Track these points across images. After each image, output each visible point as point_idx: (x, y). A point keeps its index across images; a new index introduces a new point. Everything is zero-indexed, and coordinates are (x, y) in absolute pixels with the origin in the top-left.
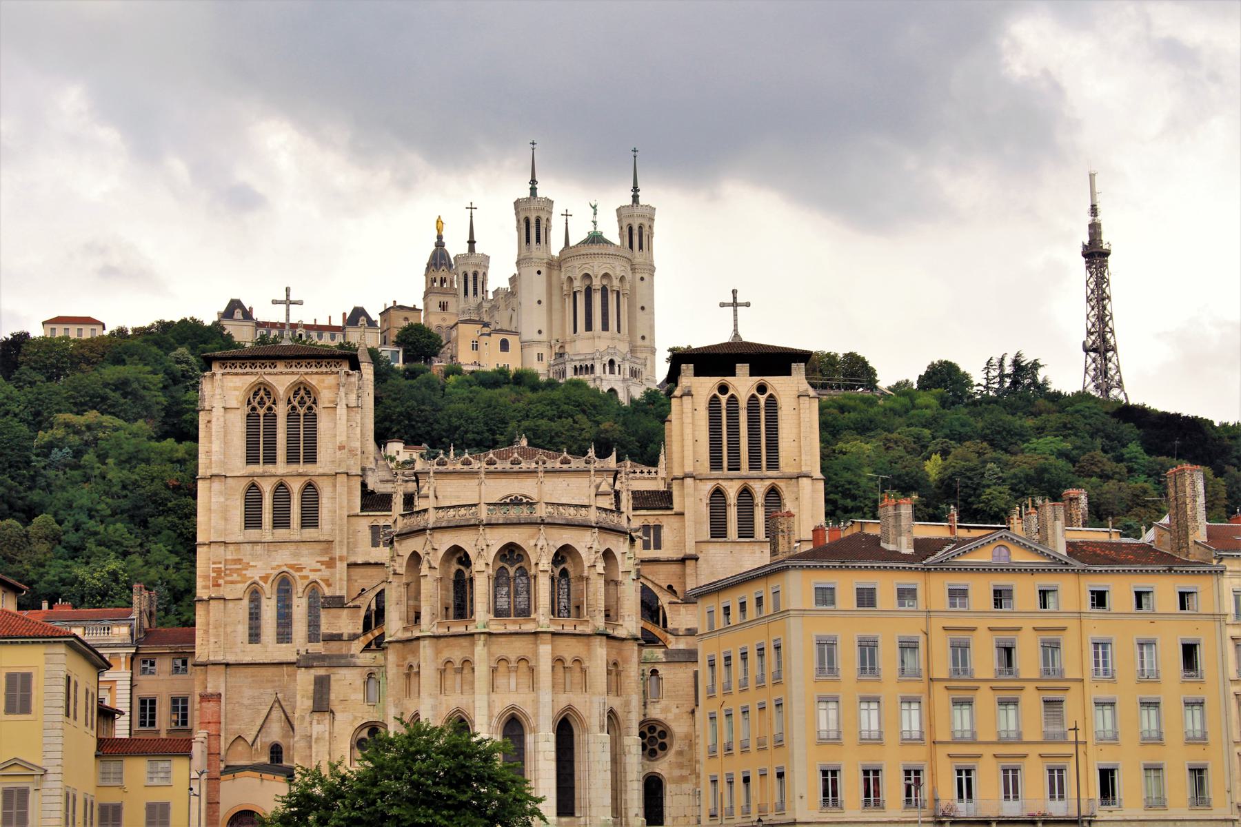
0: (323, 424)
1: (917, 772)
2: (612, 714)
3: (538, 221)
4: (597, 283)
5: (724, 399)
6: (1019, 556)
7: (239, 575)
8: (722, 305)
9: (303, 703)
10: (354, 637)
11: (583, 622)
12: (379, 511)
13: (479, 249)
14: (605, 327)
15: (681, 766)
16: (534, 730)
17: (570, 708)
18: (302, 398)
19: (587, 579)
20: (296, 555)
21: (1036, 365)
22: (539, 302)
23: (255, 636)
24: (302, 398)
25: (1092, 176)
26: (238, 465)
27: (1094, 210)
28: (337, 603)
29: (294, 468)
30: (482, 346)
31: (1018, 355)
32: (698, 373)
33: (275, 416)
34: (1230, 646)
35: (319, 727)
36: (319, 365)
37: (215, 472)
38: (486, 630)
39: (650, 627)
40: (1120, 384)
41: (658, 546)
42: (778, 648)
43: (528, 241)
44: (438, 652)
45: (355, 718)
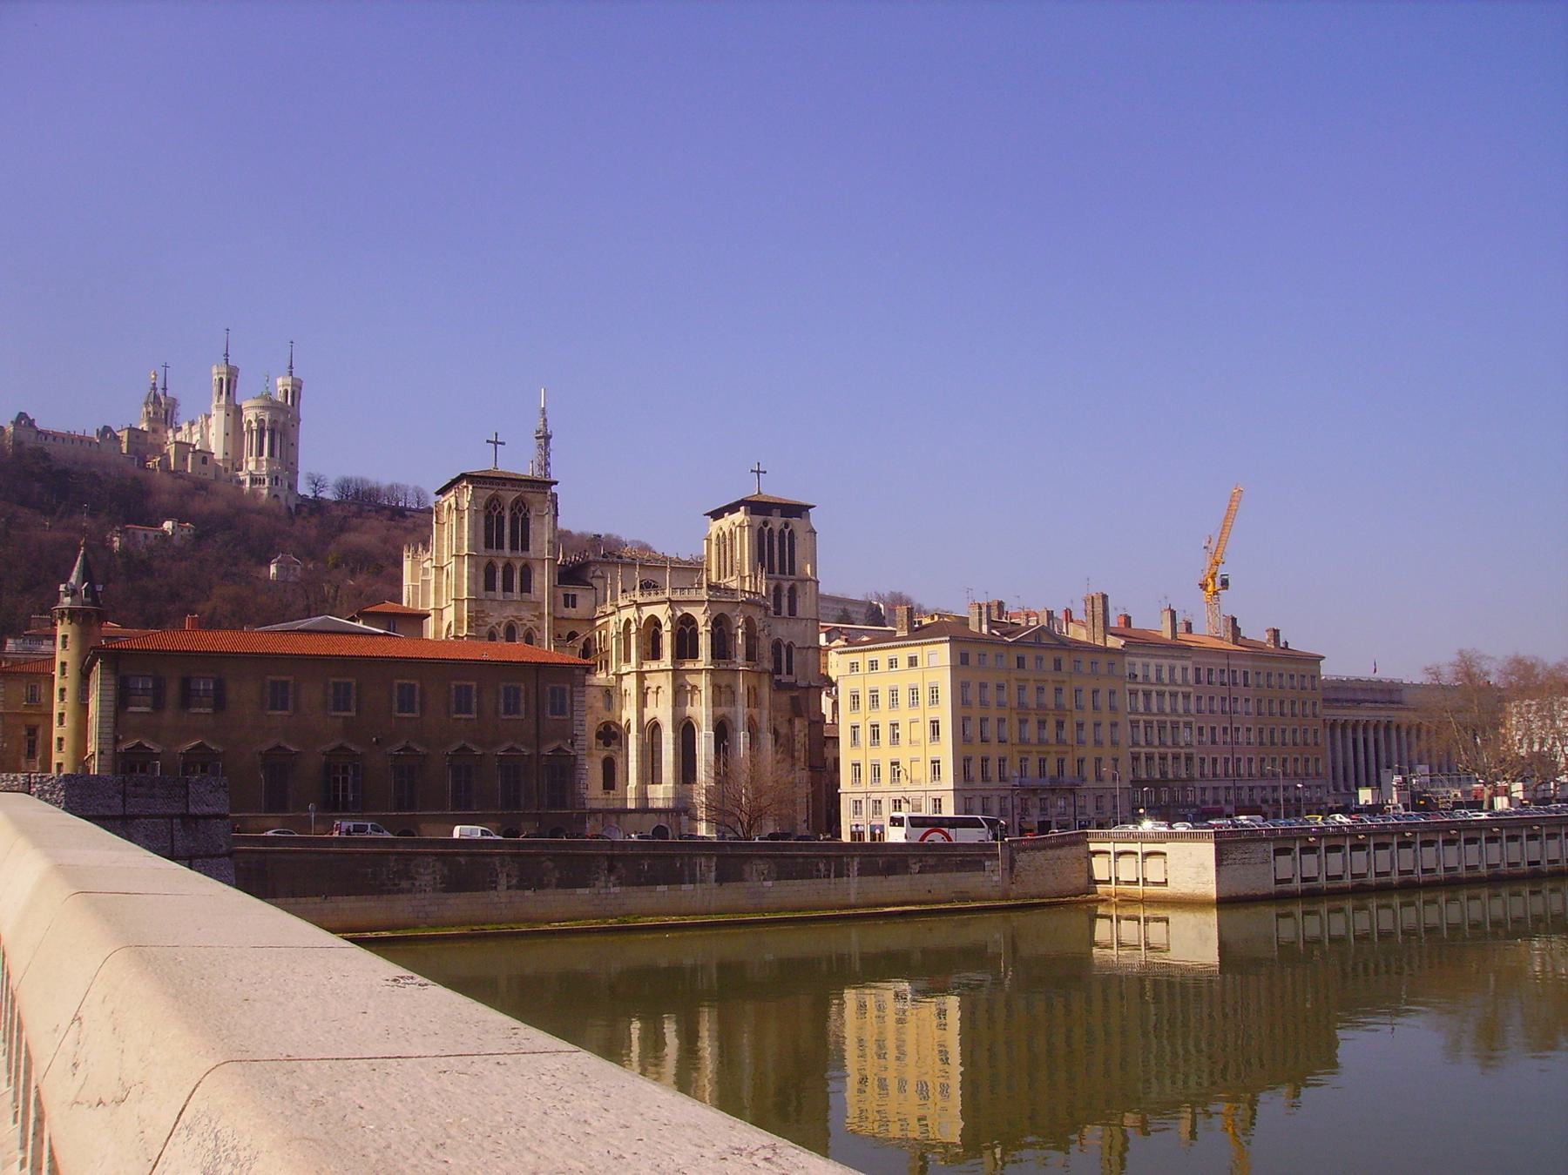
0: (533, 525)
6: (1045, 640)
22: (227, 434)
29: (515, 554)
32: (752, 514)
34: (1128, 693)
38: (712, 667)
43: (221, 393)
44: (675, 679)
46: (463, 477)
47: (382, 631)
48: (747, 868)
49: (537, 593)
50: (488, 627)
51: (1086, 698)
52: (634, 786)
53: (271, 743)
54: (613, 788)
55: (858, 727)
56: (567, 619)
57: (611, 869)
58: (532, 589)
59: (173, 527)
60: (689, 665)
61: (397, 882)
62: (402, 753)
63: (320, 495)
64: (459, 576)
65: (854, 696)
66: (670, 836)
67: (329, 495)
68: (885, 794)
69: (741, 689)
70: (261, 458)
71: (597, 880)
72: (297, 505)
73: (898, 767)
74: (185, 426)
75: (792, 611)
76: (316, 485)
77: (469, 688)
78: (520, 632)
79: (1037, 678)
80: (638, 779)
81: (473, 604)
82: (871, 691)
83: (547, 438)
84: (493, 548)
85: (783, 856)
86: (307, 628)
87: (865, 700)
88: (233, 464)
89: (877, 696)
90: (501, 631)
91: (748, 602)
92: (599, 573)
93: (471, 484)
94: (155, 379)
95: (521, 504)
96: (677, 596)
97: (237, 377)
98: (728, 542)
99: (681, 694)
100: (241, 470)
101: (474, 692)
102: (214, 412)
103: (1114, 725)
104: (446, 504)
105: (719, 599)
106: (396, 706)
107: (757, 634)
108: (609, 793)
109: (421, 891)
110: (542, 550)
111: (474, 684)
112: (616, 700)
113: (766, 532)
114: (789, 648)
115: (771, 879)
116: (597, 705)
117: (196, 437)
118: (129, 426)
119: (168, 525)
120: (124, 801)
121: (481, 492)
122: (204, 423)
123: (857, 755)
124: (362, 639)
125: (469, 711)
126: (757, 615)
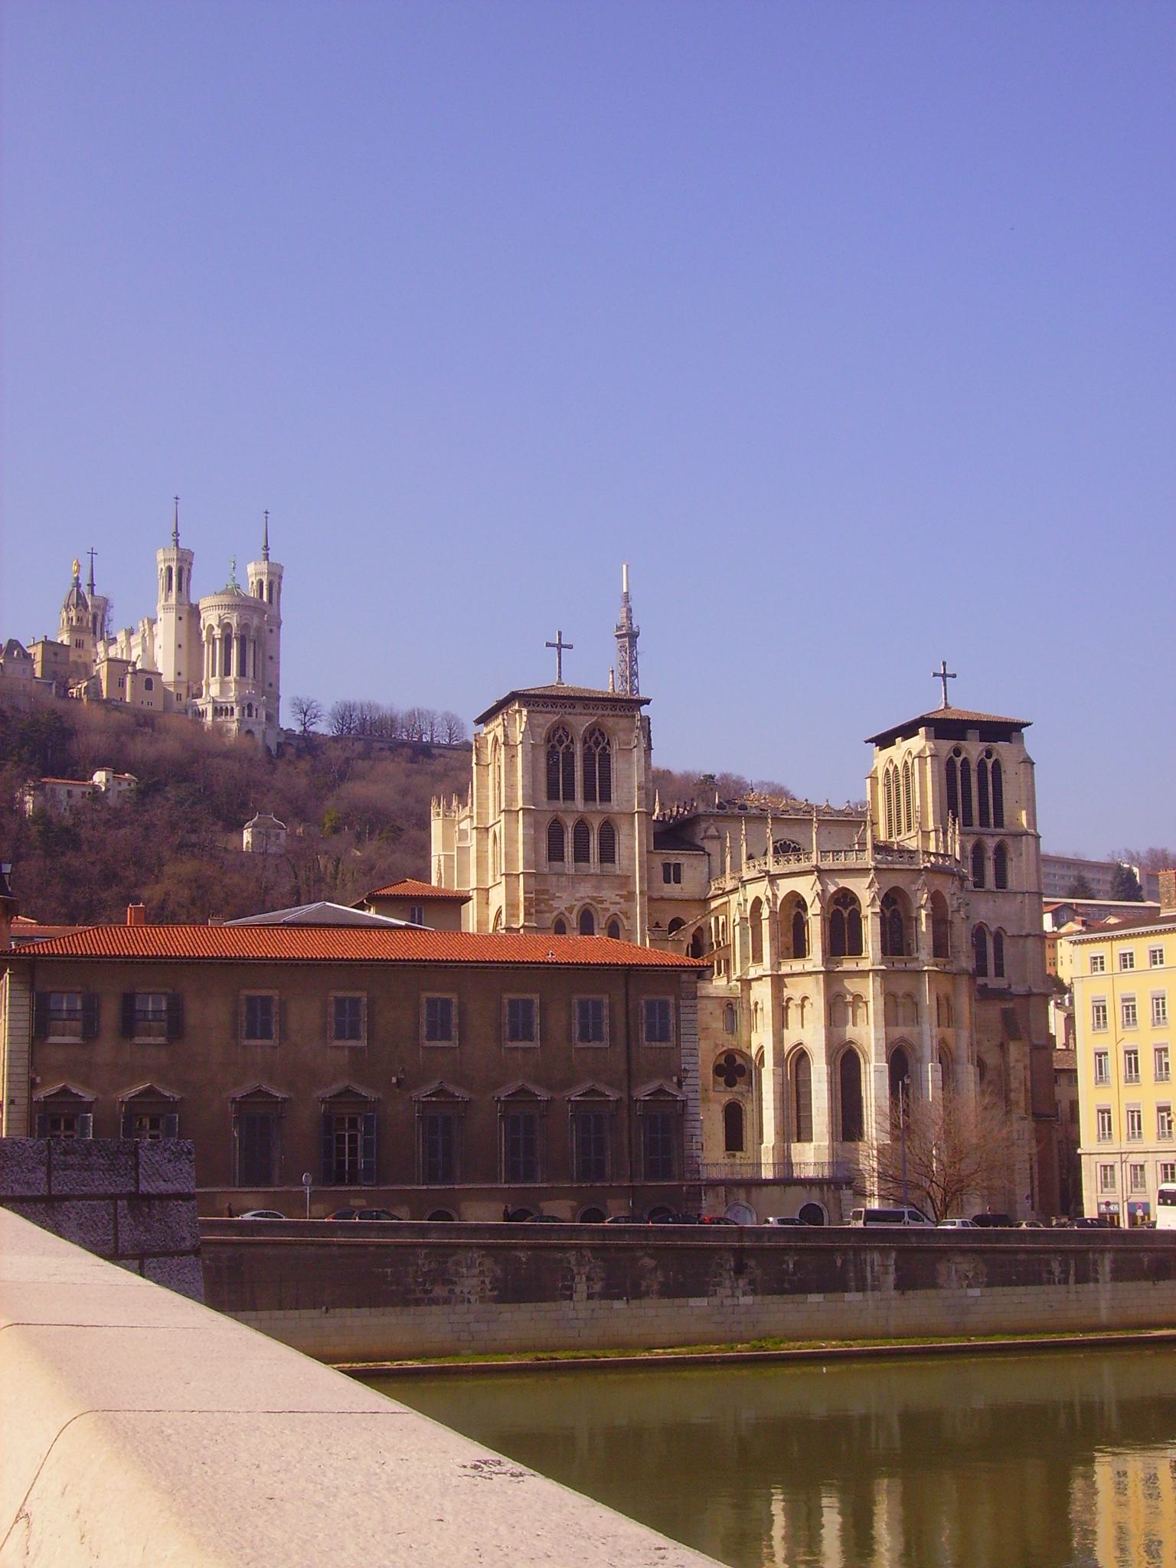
0: (617, 765)
5: (959, 761)
7: (546, 905)
8: (935, 675)
11: (948, 963)
12: (670, 849)
18: (597, 738)
19: (951, 922)
20: (597, 888)
22: (180, 646)
24: (597, 738)
25: (627, 566)
27: (627, 598)
32: (936, 738)
33: (573, 754)
36: (614, 708)
38: (883, 967)
43: (170, 588)
45: (716, 1046)
46: (514, 697)
47: (403, 923)
48: (942, 1267)
49: (625, 863)
50: (555, 913)
52: (771, 1145)
53: (249, 1086)
54: (741, 1150)
55: (1106, 1054)
56: (669, 900)
57: (740, 1270)
58: (617, 858)
59: (107, 780)
60: (848, 965)
61: (428, 1287)
62: (434, 1099)
63: (312, 728)
64: (511, 840)
65: (1098, 1008)
66: (826, 1220)
67: (323, 728)
68: (1150, 1154)
69: (928, 999)
70: (227, 679)
71: (718, 1285)
72: (279, 745)
73: (1169, 1115)
74: (121, 637)
75: (1001, 881)
76: (305, 715)
77: (529, 1004)
78: (601, 921)
80: (777, 1133)
81: (532, 881)
82: (1124, 1000)
83: (633, 636)
84: (558, 799)
85: (995, 1251)
86: (297, 921)
87: (1115, 1013)
88: (188, 688)
89: (1134, 1007)
90: (573, 919)
91: (935, 870)
92: (712, 831)
93: (525, 706)
94: (78, 571)
95: (597, 733)
96: (828, 863)
97: (191, 564)
98: (902, 781)
99: (838, 1007)
100: (200, 696)
101: (536, 1009)
102: (161, 615)
104: (490, 737)
105: (891, 866)
106: (424, 1030)
107: (949, 919)
108: (734, 1156)
109: (462, 1302)
110: (630, 801)
111: (536, 998)
112: (741, 1018)
113: (958, 764)
114: (998, 938)
115: (978, 1285)
116: (714, 1025)
117: (137, 652)
118: (44, 639)
119: (99, 777)
120: (49, 1174)
121: (540, 719)
122: (147, 632)
123: (1105, 1097)
124: (375, 935)
125: (529, 1037)
126: (948, 888)
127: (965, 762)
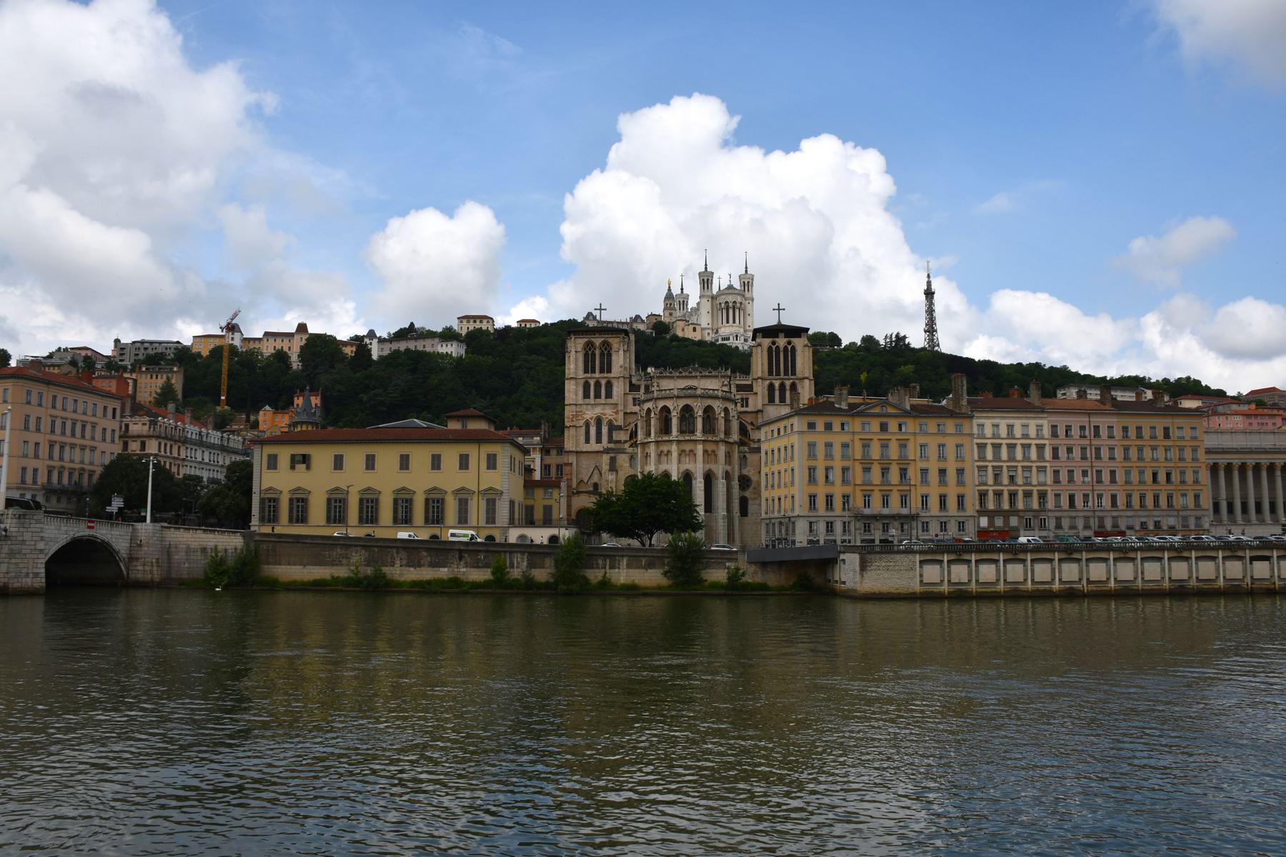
0: (614, 358)
1: (848, 497)
2: (727, 473)
3: (708, 280)
4: (731, 305)
5: (774, 347)
6: (891, 410)
9: (605, 467)
10: (626, 442)
13: (685, 292)
14: (734, 322)
15: (755, 493)
16: (696, 479)
17: (710, 470)
21: (905, 337)
23: (587, 441)
26: (581, 374)
28: (619, 428)
29: (602, 375)
30: (686, 330)
31: (898, 333)
32: (763, 337)
34: (975, 447)
35: (611, 477)
37: (572, 376)
39: (743, 438)
40: (938, 345)
41: (747, 406)
42: (792, 446)
51: (932, 452)
57: (460, 558)
79: (861, 437)
103: (960, 472)
127: (778, 348)
